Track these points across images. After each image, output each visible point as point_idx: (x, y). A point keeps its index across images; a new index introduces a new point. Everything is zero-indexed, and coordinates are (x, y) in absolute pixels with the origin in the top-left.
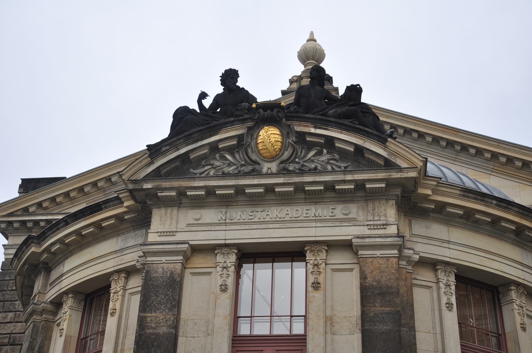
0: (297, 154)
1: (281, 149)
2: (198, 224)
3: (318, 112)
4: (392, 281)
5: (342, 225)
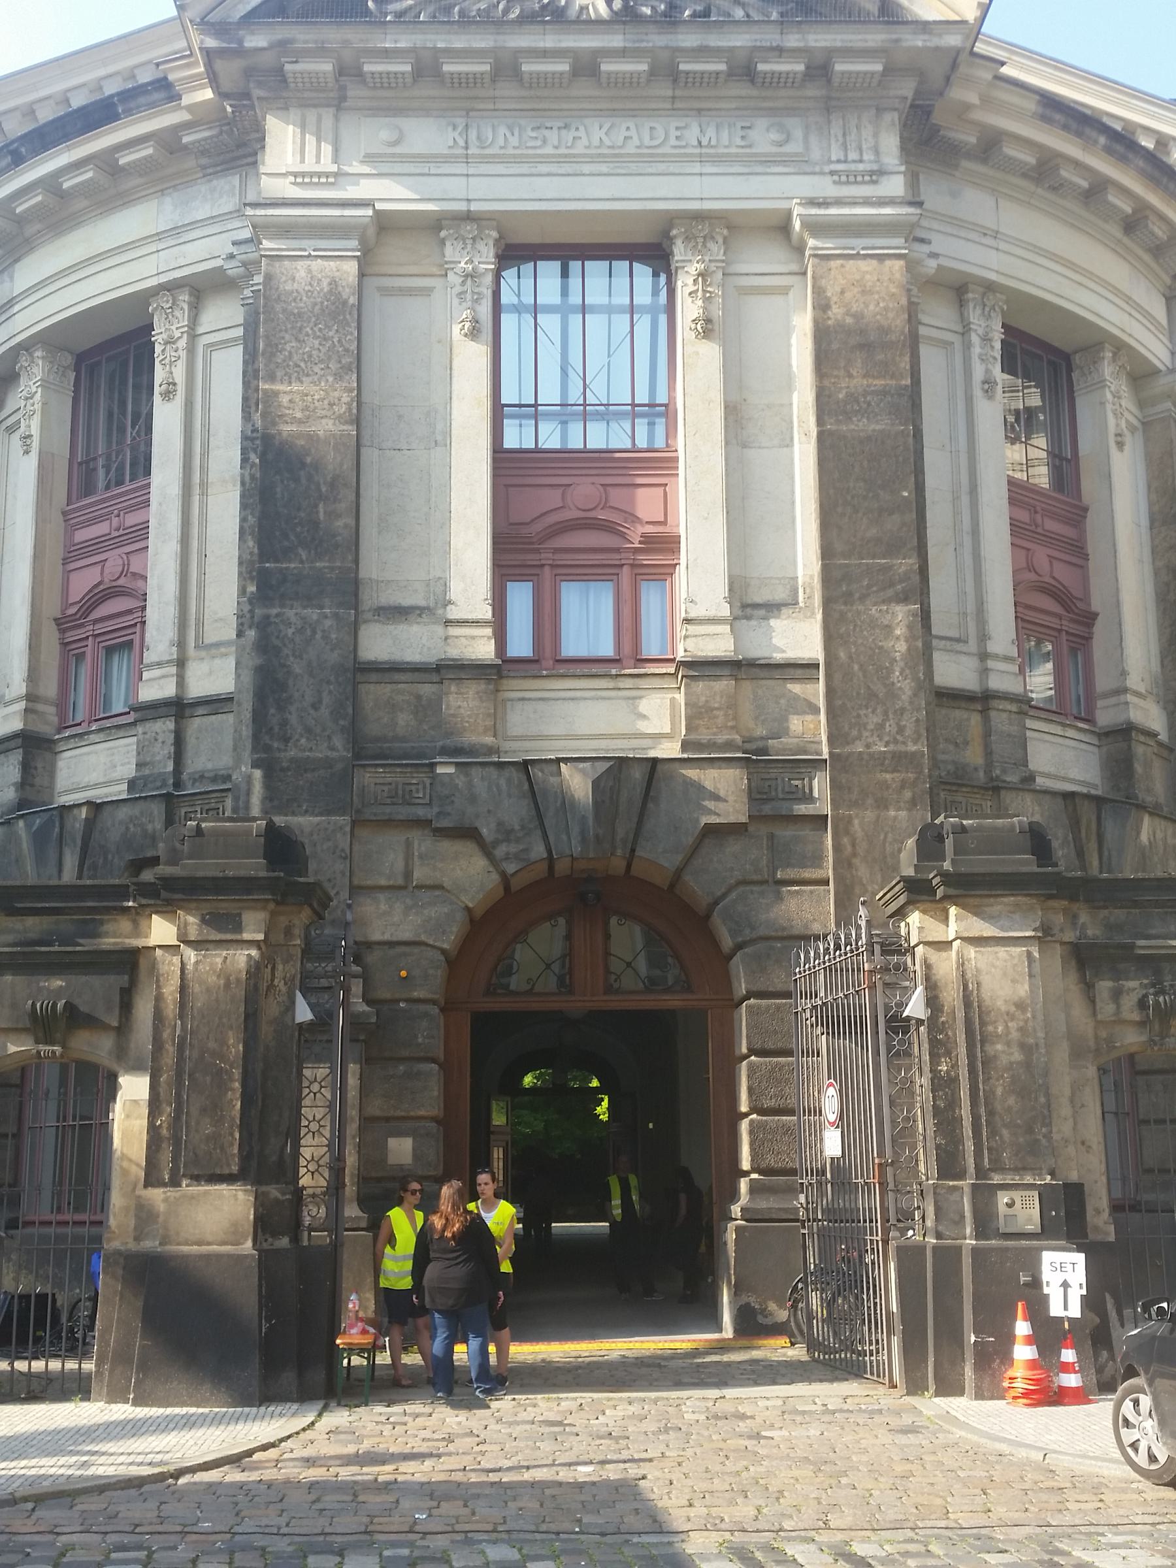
2: (393, 155)
4: (891, 315)
5: (769, 170)
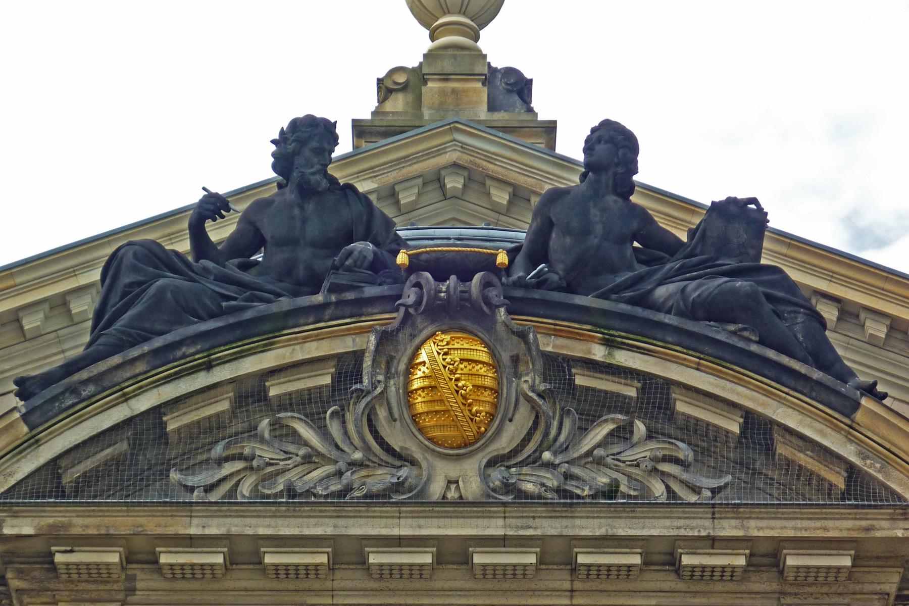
0: (546, 434)
1: (492, 416)
3: (618, 289)
